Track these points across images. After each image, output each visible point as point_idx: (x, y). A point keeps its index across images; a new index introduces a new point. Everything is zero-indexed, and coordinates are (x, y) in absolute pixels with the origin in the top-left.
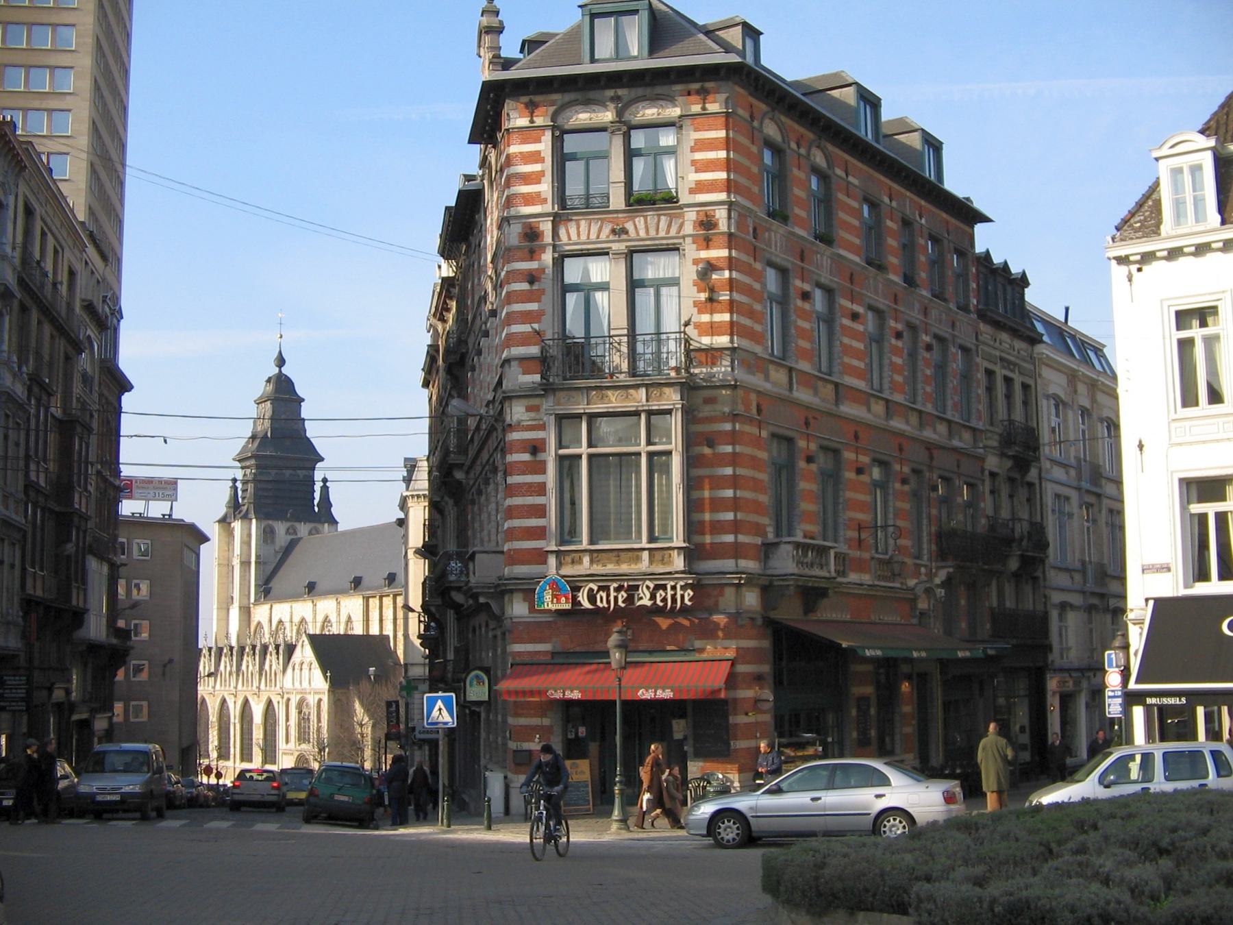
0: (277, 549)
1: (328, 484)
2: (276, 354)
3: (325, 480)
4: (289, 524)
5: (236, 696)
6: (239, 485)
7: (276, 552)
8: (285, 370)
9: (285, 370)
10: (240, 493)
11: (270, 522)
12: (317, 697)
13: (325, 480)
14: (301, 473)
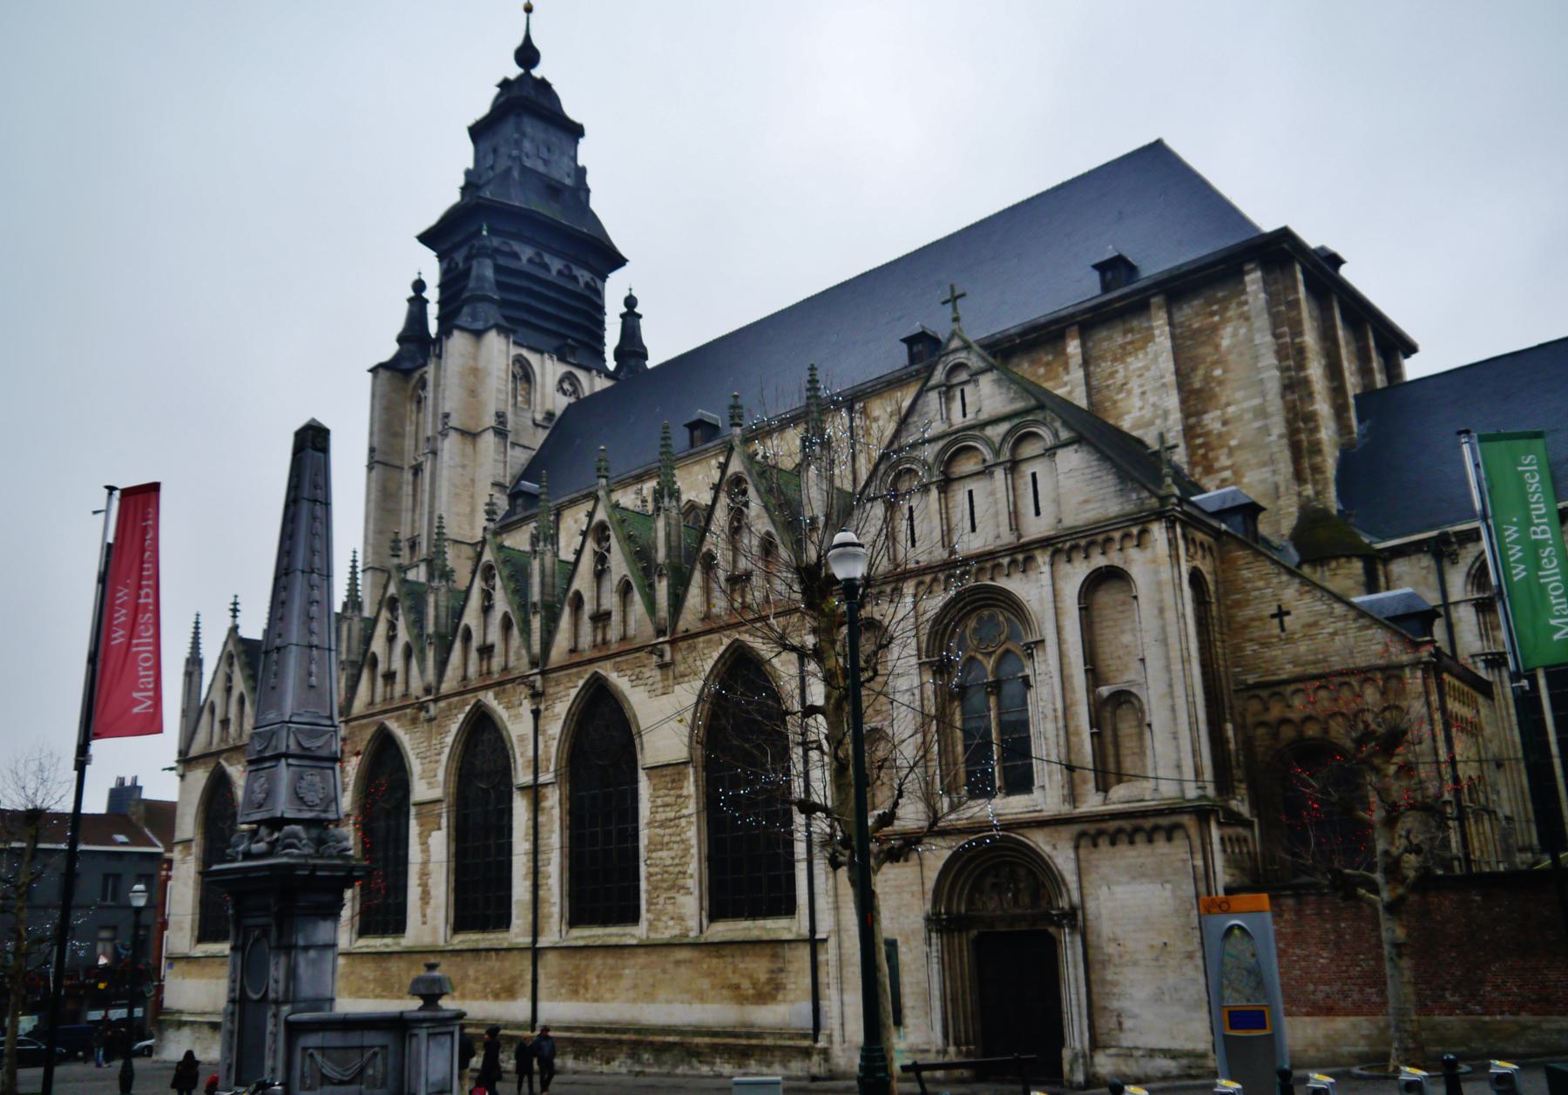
0: (539, 417)
1: (637, 310)
2: (518, 41)
3: (630, 302)
4: (562, 369)
5: (536, 696)
6: (432, 294)
7: (536, 425)
8: (537, 73)
9: (537, 73)
10: (433, 310)
11: (525, 353)
12: (1076, 573)
13: (630, 302)
14: (583, 276)
